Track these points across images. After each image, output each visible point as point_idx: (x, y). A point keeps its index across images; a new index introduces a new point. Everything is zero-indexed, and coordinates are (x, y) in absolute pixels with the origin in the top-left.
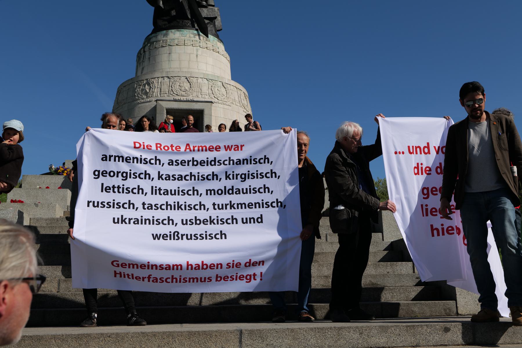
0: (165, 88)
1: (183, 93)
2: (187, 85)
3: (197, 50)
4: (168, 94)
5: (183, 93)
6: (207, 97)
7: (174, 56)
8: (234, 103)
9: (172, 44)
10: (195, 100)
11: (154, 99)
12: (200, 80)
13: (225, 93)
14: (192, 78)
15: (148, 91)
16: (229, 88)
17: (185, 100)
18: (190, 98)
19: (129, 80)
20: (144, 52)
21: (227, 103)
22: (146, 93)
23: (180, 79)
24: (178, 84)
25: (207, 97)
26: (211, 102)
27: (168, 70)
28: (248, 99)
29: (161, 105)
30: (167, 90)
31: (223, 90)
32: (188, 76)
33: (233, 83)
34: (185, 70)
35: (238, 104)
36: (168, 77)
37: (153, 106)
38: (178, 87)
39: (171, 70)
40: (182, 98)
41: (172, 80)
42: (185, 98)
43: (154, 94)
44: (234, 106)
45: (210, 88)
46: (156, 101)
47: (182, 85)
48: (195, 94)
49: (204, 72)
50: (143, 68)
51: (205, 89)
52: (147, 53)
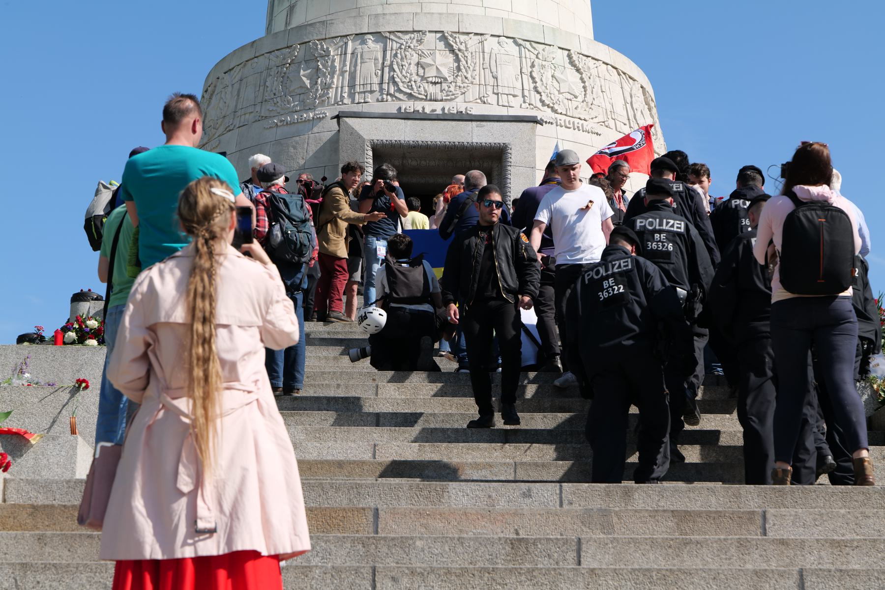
0: (369, 72)
1: (432, 90)
2: (444, 62)
4: (377, 95)
5: (432, 90)
6: (516, 102)
8: (611, 123)
10: (474, 112)
11: (330, 111)
12: (491, 44)
13: (578, 89)
14: (463, 38)
15: (307, 82)
16: (594, 72)
17: (439, 112)
18: (458, 105)
19: (243, 48)
21: (588, 125)
23: (420, 41)
24: (415, 58)
25: (516, 102)
26: (534, 121)
27: (379, 10)
28: (654, 111)
29: (353, 132)
30: (376, 80)
31: (572, 76)
32: (448, 28)
33: (604, 52)
36: (379, 36)
37: (327, 136)
38: (413, 69)
39: (389, 10)
40: (429, 107)
42: (438, 107)
43: (332, 93)
45: (527, 70)
46: (338, 117)
47: (429, 60)
48: (473, 93)
49: (505, 15)
51: (509, 75)
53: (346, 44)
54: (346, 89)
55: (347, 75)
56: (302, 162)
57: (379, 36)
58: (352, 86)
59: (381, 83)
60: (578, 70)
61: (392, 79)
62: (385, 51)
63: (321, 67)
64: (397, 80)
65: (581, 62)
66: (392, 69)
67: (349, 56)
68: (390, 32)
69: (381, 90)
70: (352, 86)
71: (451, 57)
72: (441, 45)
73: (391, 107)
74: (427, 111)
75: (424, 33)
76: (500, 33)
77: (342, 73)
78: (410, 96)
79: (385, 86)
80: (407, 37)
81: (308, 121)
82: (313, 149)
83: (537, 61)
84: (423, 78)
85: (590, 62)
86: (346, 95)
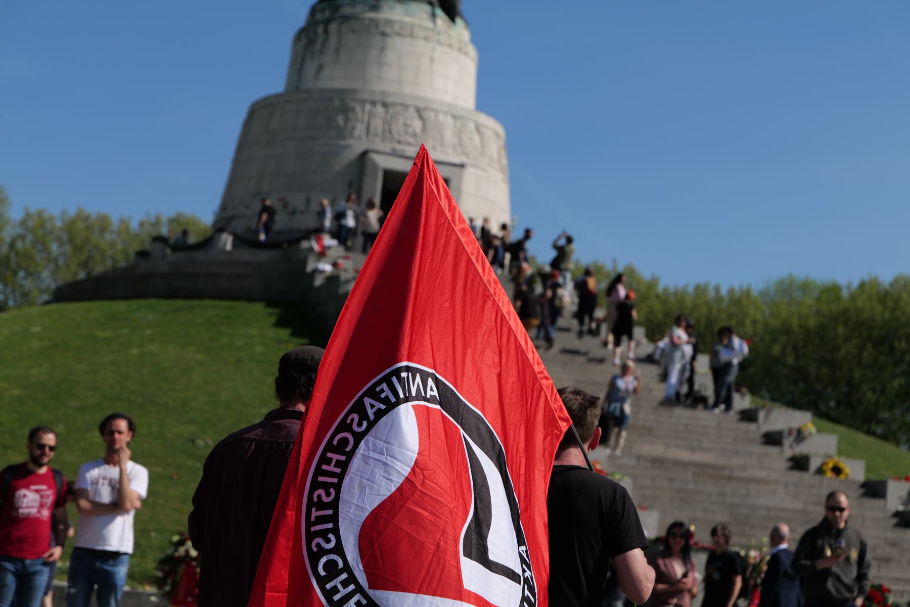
0: (377, 124)
1: (411, 140)
2: (417, 124)
3: (433, 49)
5: (411, 140)
7: (390, 56)
9: (388, 30)
12: (441, 117)
20: (326, 32)
26: (462, 166)
31: (477, 138)
32: (421, 105)
34: (408, 90)
36: (385, 105)
41: (391, 111)
47: (409, 122)
50: (320, 68)
51: (449, 135)
52: (333, 39)
57: (385, 105)
58: (368, 129)
59: (384, 131)
61: (390, 132)
65: (483, 130)
70: (368, 129)
72: (415, 115)
73: (387, 147)
78: (399, 142)
84: (406, 132)
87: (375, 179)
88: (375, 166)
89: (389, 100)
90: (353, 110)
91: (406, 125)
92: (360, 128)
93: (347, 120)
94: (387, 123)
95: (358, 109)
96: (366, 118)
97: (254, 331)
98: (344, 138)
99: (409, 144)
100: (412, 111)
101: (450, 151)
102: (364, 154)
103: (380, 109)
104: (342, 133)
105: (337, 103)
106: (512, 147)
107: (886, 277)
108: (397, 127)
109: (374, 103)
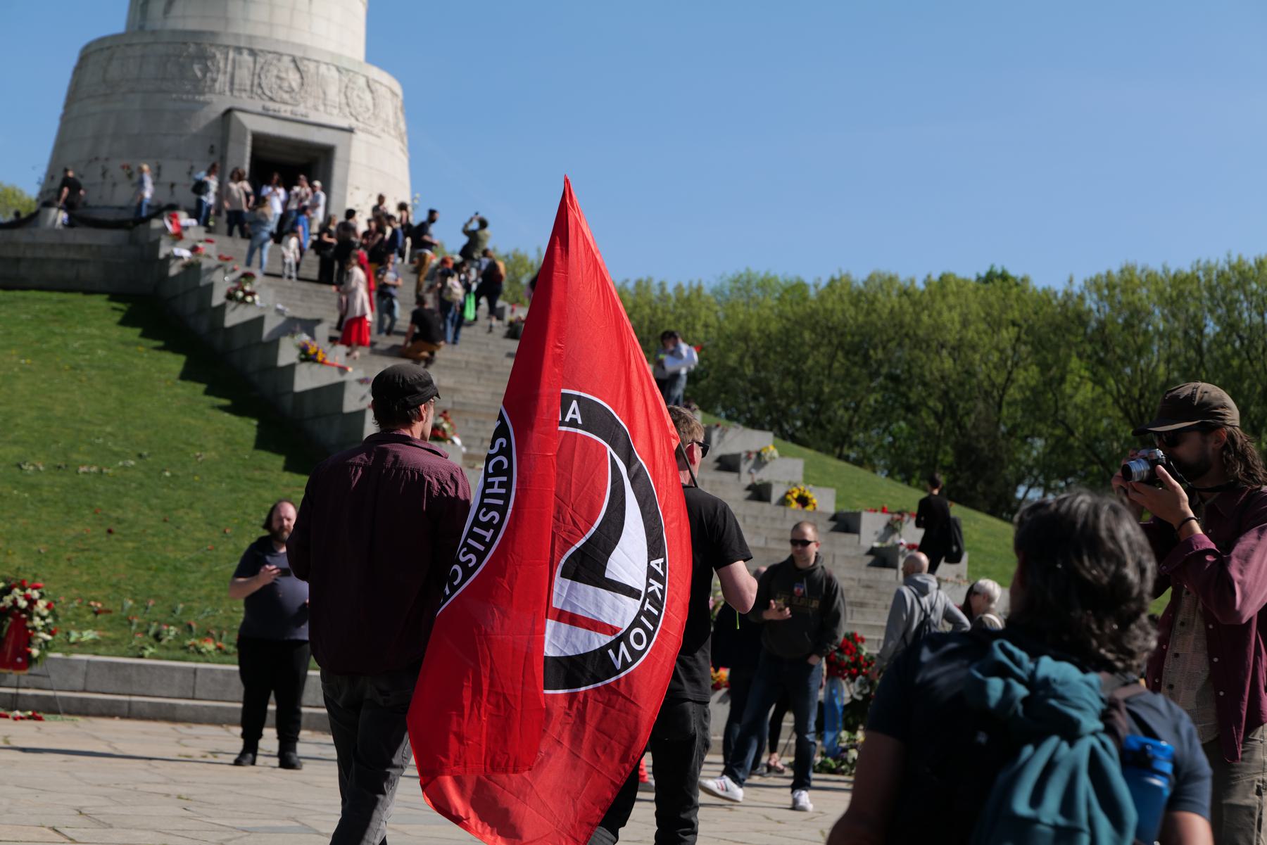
0: (244, 76)
1: (286, 97)
2: (293, 78)
5: (286, 97)
12: (323, 68)
13: (371, 107)
14: (306, 62)
15: (199, 74)
17: (288, 115)
18: (301, 109)
22: (196, 81)
23: (279, 60)
24: (275, 72)
26: (351, 130)
30: (248, 83)
31: (368, 96)
32: (298, 54)
34: (281, 34)
35: (393, 132)
36: (253, 53)
38: (274, 80)
40: (286, 111)
41: (261, 60)
43: (217, 86)
44: (385, 136)
47: (283, 75)
48: (310, 103)
51: (333, 92)
53: (227, 54)
54: (228, 85)
55: (228, 76)
56: (194, 130)
57: (253, 53)
58: (232, 83)
59: (252, 85)
60: (372, 91)
61: (260, 85)
62: (255, 62)
63: (209, 63)
64: (264, 85)
65: (375, 86)
66: (259, 77)
67: (230, 62)
68: (262, 51)
69: (252, 91)
70: (232, 83)
71: (297, 76)
72: (292, 65)
73: (257, 105)
74: (283, 114)
75: (281, 55)
76: (328, 60)
77: (225, 73)
78: (271, 99)
79: (255, 88)
80: (270, 56)
81: (198, 102)
82: (203, 123)
83: (351, 85)
84: (280, 87)
85: (378, 86)
86: (227, 89)
87: (244, 144)
88: (242, 127)
89: (256, 47)
90: (214, 56)
91: (278, 77)
92: (222, 80)
93: (206, 70)
94: (256, 75)
95: (219, 56)
96: (229, 68)
97: (95, 331)
98: (203, 93)
99: (285, 103)
100: (286, 59)
101: (336, 111)
102: (229, 112)
103: (246, 58)
104: (199, 86)
105: (192, 49)
106: (411, 108)
107: (859, 275)
108: (269, 81)
109: (239, 50)
